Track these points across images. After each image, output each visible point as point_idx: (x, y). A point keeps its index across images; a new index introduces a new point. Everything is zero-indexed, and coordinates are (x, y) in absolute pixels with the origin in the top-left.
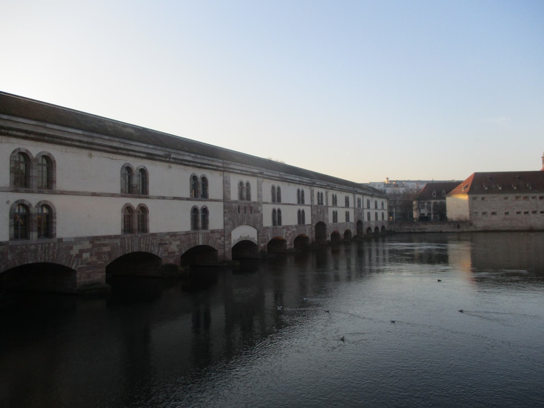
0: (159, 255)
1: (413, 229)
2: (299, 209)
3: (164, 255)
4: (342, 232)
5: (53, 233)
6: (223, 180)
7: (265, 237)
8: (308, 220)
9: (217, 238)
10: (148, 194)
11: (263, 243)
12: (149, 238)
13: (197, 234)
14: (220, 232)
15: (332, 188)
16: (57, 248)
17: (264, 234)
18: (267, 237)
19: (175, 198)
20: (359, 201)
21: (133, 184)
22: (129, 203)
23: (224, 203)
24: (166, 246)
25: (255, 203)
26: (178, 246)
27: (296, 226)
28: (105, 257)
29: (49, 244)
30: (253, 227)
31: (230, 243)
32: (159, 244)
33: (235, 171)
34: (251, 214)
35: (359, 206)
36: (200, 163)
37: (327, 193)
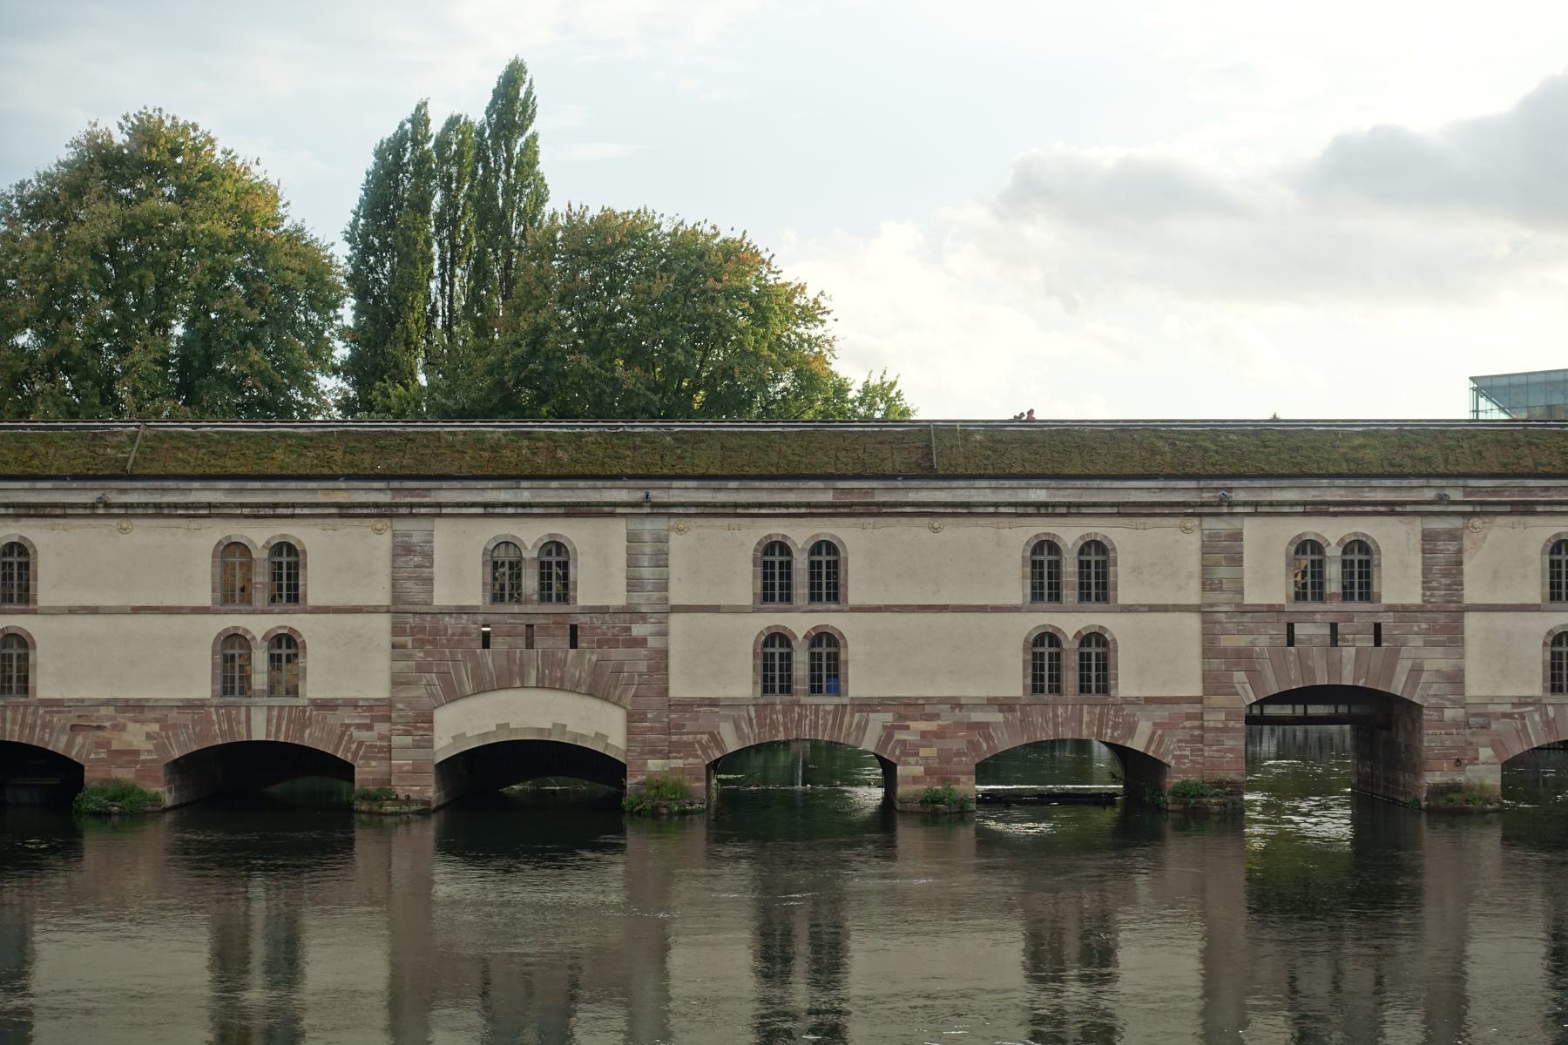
0: (73, 755)
3: (92, 756)
9: (349, 726)
10: (35, 602)
14: (370, 708)
18: (705, 737)
24: (100, 733)
25: (603, 610)
26: (149, 736)
31: (429, 744)
32: (73, 727)
34: (572, 652)
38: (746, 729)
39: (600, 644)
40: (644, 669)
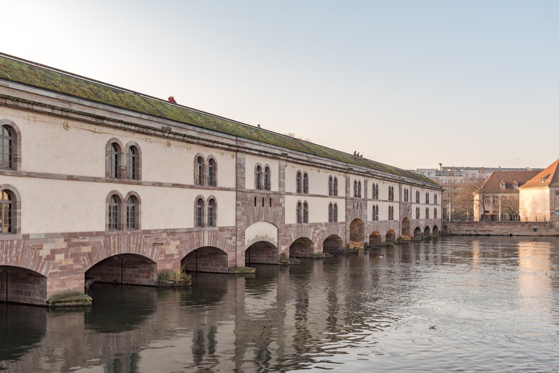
0: (153, 259)
1: (474, 231)
2: (330, 202)
3: (160, 259)
4: (383, 233)
5: (18, 227)
6: (236, 162)
7: (287, 238)
8: (341, 217)
9: (226, 238)
11: (284, 245)
12: (141, 236)
13: (202, 232)
15: (373, 176)
16: (22, 247)
17: (286, 234)
18: (289, 237)
19: (174, 185)
20: (406, 192)
21: (122, 165)
22: (116, 191)
23: (237, 193)
24: (163, 247)
25: (275, 193)
26: (177, 247)
27: (326, 224)
28: (84, 260)
29: (12, 241)
30: (273, 224)
32: (154, 244)
33: (252, 151)
35: (406, 199)
36: (207, 140)
37: (366, 182)
38: (295, 235)
39: (275, 205)
40: (281, 215)
